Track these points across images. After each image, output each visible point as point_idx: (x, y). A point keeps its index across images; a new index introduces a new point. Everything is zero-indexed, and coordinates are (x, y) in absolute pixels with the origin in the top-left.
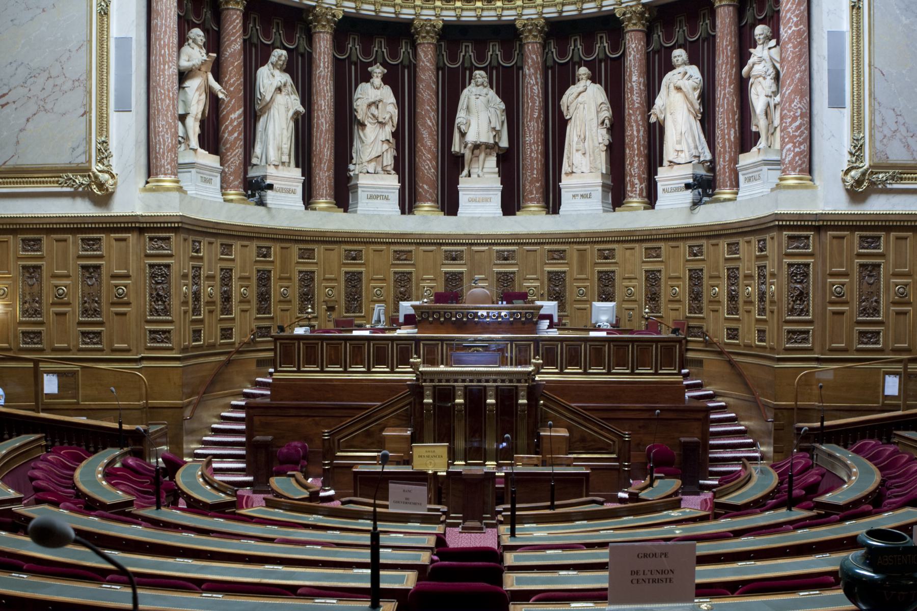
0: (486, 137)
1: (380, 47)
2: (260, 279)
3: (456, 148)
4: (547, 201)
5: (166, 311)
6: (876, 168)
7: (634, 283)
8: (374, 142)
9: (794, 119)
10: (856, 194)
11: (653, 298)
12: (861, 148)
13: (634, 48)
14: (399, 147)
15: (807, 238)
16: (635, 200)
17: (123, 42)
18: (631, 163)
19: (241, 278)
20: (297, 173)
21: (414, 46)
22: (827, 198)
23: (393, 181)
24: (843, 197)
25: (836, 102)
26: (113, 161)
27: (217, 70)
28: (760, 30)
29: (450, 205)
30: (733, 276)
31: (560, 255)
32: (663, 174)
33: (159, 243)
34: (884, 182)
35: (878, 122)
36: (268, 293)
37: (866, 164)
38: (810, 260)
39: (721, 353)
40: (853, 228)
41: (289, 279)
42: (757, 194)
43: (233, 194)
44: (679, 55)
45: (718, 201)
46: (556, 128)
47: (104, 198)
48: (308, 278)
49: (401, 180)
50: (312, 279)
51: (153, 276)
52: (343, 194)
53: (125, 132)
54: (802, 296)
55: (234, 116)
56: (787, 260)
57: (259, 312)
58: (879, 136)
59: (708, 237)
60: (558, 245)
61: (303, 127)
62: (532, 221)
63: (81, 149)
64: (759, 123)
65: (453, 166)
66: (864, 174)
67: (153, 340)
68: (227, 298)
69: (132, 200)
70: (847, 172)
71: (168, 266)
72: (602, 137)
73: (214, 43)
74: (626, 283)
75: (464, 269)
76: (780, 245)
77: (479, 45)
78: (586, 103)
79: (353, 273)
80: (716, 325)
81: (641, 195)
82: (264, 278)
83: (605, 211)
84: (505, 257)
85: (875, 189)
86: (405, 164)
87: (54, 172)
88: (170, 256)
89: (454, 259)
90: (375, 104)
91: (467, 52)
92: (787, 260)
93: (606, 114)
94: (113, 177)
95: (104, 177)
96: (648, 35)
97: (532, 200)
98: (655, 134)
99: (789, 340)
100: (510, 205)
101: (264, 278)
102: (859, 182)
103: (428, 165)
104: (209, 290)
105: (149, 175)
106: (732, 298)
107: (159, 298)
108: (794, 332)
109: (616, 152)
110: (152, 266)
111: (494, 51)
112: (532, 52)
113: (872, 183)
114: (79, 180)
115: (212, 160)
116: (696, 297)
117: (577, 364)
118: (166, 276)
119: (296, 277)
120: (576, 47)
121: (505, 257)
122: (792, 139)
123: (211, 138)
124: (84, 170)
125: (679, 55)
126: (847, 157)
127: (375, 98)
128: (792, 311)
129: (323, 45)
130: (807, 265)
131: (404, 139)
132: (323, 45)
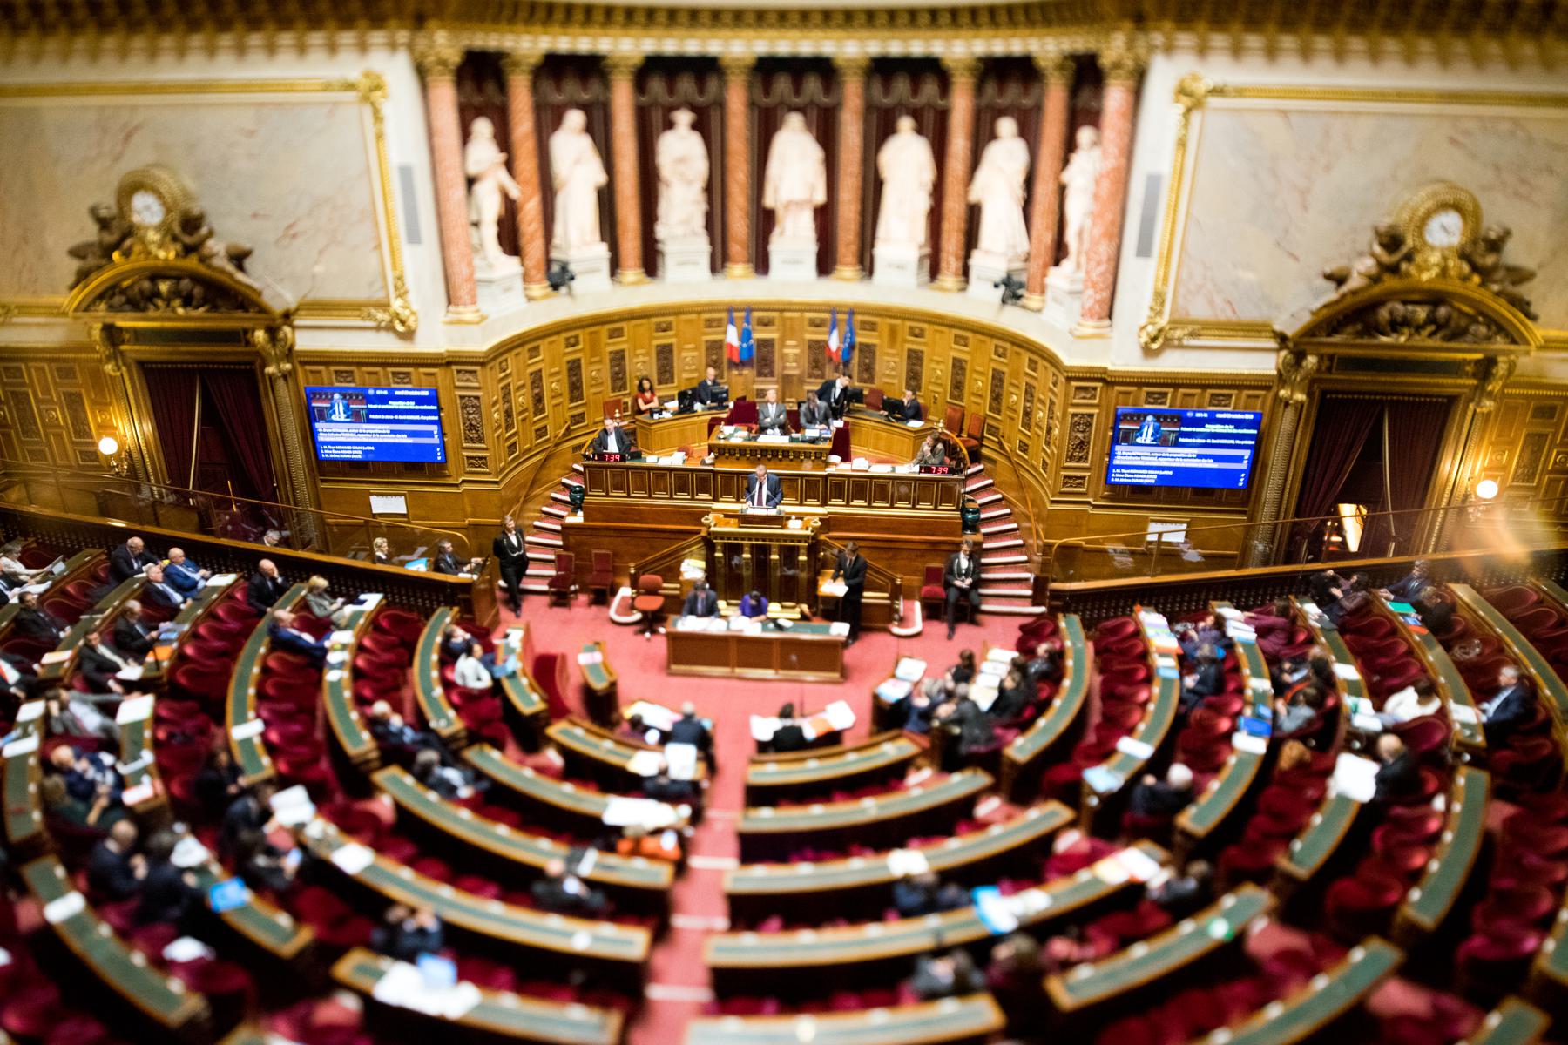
0: (799, 193)
1: (686, 85)
2: (570, 370)
3: (769, 202)
4: (861, 261)
5: (480, 440)
6: (1175, 323)
7: (942, 367)
8: (682, 207)
9: (1099, 264)
10: (1147, 351)
11: (958, 386)
12: (1162, 304)
13: (961, 106)
14: (710, 201)
15: (1095, 389)
16: (949, 279)
17: (406, 173)
18: (952, 234)
19: (552, 375)
20: (603, 250)
21: (723, 84)
22: (1120, 353)
23: (702, 246)
24: (1138, 352)
25: (1144, 250)
26: (411, 297)
27: (509, 166)
28: (1085, 135)
29: (761, 264)
30: (1029, 392)
31: (872, 327)
32: (977, 259)
33: (468, 376)
34: (1180, 339)
35: (1184, 276)
36: (580, 381)
37: (1163, 321)
38: (1095, 411)
39: (1009, 459)
40: (1140, 385)
41: (600, 362)
42: (1059, 324)
43: (540, 288)
44: (1007, 126)
45: (1024, 307)
46: (873, 189)
47: (408, 335)
48: (618, 358)
49: (712, 243)
50: (623, 358)
51: (464, 407)
52: (651, 261)
53: (419, 266)
54: (1082, 445)
55: (530, 211)
56: (1072, 410)
57: (572, 400)
58: (1182, 290)
59: (1013, 344)
60: (872, 317)
61: (606, 199)
62: (845, 288)
63: (378, 285)
64: (1071, 237)
65: (765, 221)
66: (1160, 331)
67: (472, 465)
68: (538, 399)
69: (434, 338)
70: (1143, 328)
71: (477, 398)
72: (923, 203)
73: (503, 140)
74: (934, 365)
75: (775, 336)
76: (1067, 395)
77: (794, 84)
78: (906, 159)
79: (664, 346)
80: (1014, 433)
81: (956, 275)
82: (574, 368)
83: (920, 285)
84: (816, 324)
85: (1168, 344)
86: (715, 224)
87: (355, 307)
88: (478, 388)
89: (766, 325)
90: (682, 160)
91: (782, 85)
92: (1072, 410)
93: (928, 174)
94: (413, 313)
95: (405, 313)
96: (979, 89)
97: (847, 265)
98: (973, 214)
99: (1065, 484)
100: (825, 264)
101: (574, 368)
102: (1154, 339)
103: (739, 225)
104: (521, 399)
105: (450, 302)
106: (1027, 414)
107: (472, 427)
108: (1070, 477)
109: (935, 217)
110: (462, 397)
111: (812, 85)
112: (852, 96)
113: (1166, 339)
114: (380, 315)
115: (512, 264)
116: (996, 398)
117: (862, 498)
118: (477, 407)
119: (607, 359)
120: (902, 86)
121: (816, 324)
122: (1094, 285)
123: (510, 239)
124: (384, 306)
125: (1007, 126)
126: (1147, 312)
127: (681, 150)
128: (1071, 458)
129: (623, 99)
130: (1091, 416)
131: (715, 190)
132: (623, 99)
